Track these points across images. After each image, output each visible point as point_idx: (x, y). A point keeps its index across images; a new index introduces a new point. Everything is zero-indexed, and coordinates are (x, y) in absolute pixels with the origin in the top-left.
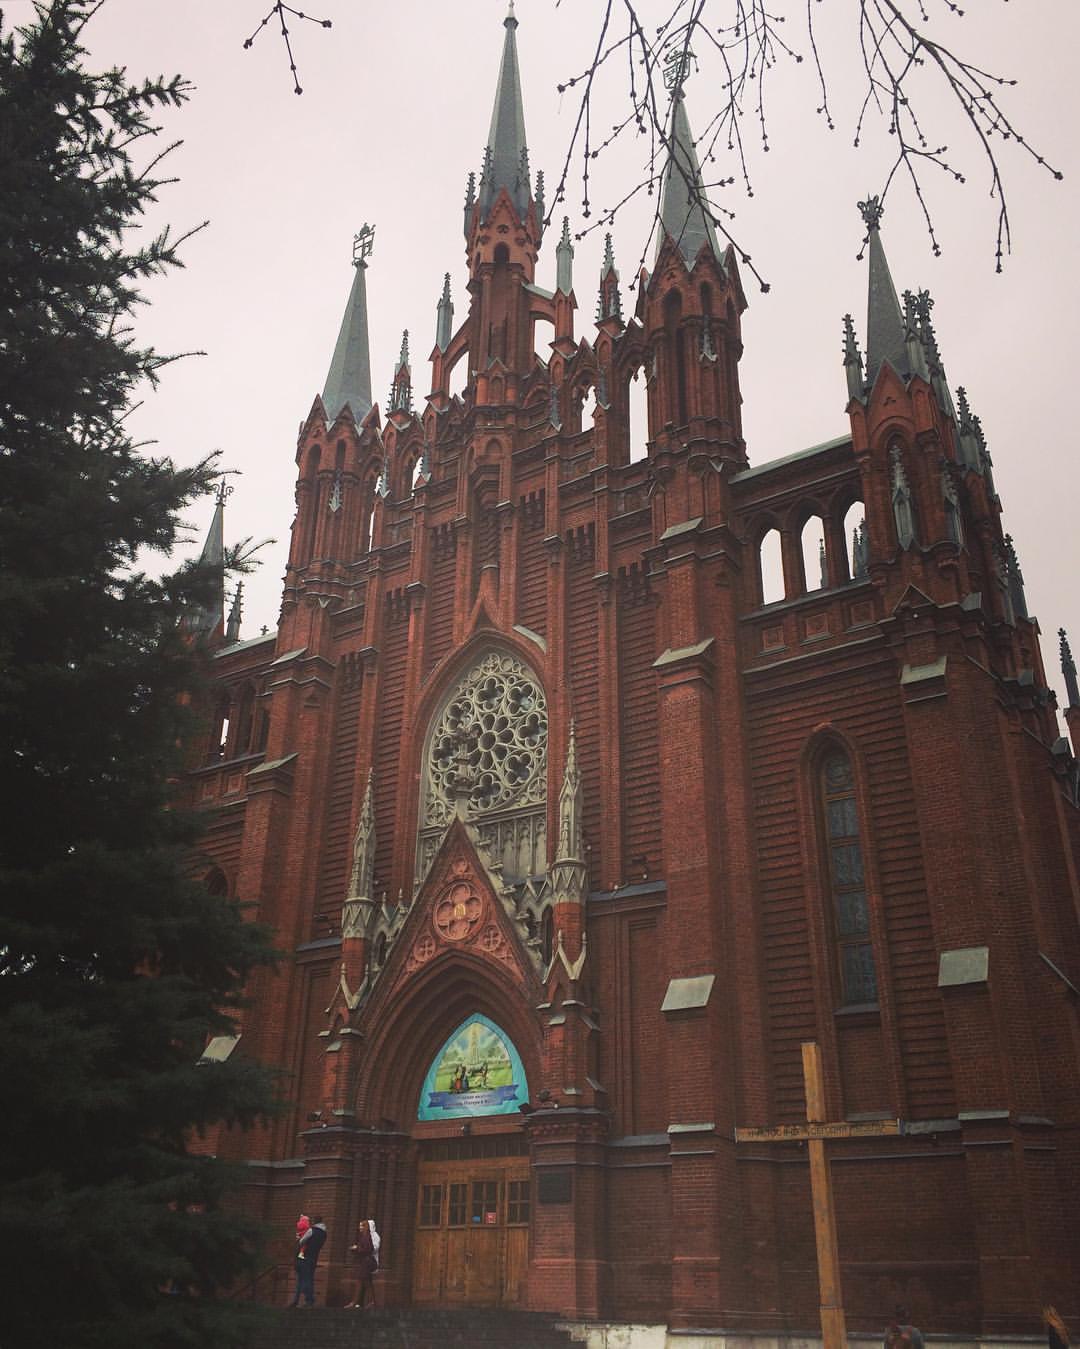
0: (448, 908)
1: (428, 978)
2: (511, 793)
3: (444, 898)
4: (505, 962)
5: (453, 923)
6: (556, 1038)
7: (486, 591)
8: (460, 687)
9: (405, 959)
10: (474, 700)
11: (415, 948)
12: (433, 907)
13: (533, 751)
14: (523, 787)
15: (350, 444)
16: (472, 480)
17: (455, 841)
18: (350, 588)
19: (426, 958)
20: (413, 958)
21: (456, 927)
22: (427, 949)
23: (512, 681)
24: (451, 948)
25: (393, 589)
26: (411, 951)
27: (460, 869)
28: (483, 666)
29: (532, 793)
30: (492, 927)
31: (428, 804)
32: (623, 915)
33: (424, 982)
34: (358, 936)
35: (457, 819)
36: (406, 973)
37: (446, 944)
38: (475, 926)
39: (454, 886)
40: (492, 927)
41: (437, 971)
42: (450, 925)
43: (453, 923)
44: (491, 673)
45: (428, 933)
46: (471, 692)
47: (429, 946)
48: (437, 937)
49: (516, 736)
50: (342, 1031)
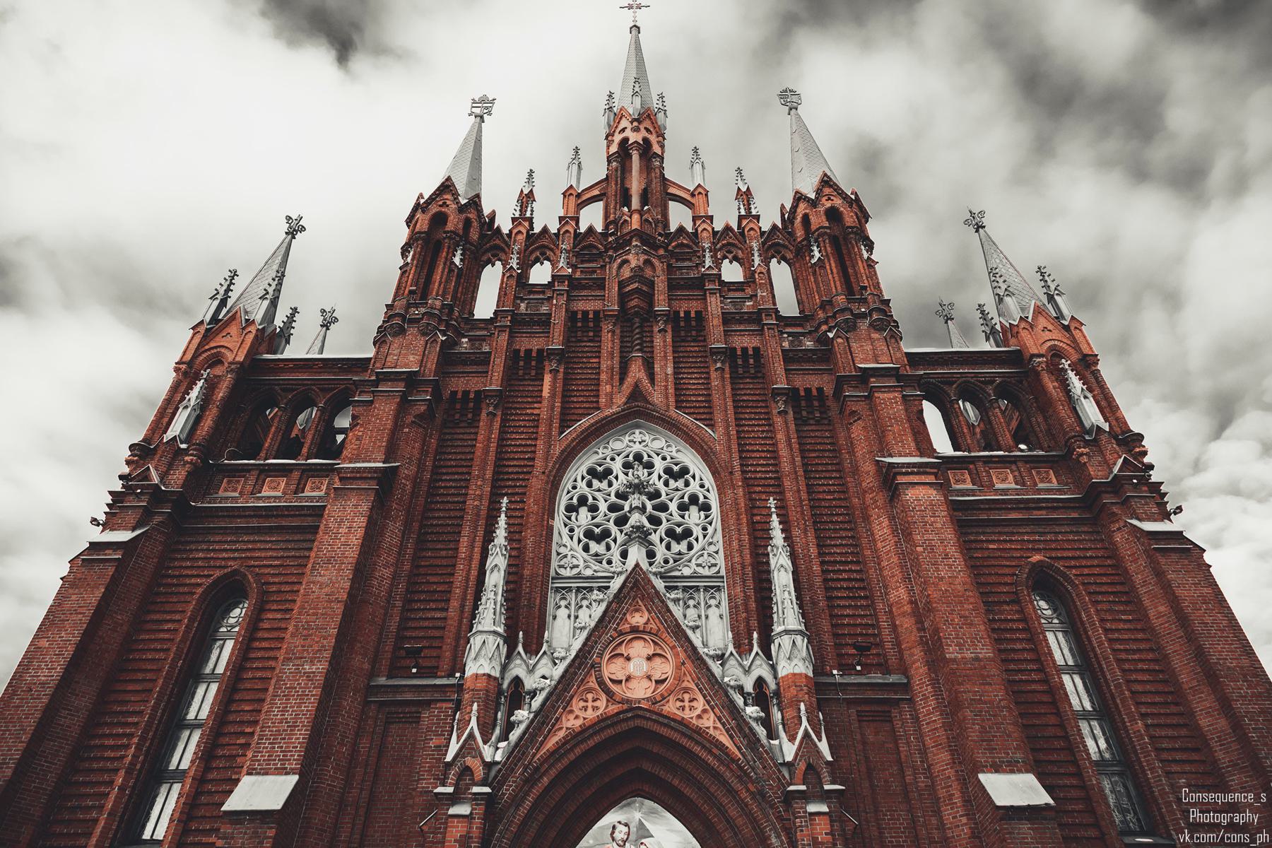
1: (597, 739)
4: (711, 732)
5: (628, 679)
6: (822, 830)
7: (637, 372)
8: (600, 451)
10: (617, 467)
11: (574, 701)
12: (601, 655)
13: (698, 525)
14: (687, 557)
15: (475, 224)
16: (621, 285)
17: (632, 588)
18: (465, 337)
19: (590, 714)
20: (571, 712)
21: (632, 684)
22: (590, 704)
23: (664, 459)
24: (632, 710)
25: (523, 349)
26: (569, 703)
27: (638, 619)
28: (627, 438)
29: (698, 565)
30: (686, 690)
31: (558, 554)
32: (850, 702)
33: (591, 743)
34: (493, 674)
35: (637, 565)
36: (561, 728)
37: (622, 701)
38: (662, 687)
39: (630, 637)
40: (686, 690)
41: (611, 732)
42: (627, 680)
43: (628, 679)
44: (637, 448)
45: (592, 683)
46: (613, 459)
47: (594, 700)
48: (610, 694)
49: (673, 507)
50: (476, 789)
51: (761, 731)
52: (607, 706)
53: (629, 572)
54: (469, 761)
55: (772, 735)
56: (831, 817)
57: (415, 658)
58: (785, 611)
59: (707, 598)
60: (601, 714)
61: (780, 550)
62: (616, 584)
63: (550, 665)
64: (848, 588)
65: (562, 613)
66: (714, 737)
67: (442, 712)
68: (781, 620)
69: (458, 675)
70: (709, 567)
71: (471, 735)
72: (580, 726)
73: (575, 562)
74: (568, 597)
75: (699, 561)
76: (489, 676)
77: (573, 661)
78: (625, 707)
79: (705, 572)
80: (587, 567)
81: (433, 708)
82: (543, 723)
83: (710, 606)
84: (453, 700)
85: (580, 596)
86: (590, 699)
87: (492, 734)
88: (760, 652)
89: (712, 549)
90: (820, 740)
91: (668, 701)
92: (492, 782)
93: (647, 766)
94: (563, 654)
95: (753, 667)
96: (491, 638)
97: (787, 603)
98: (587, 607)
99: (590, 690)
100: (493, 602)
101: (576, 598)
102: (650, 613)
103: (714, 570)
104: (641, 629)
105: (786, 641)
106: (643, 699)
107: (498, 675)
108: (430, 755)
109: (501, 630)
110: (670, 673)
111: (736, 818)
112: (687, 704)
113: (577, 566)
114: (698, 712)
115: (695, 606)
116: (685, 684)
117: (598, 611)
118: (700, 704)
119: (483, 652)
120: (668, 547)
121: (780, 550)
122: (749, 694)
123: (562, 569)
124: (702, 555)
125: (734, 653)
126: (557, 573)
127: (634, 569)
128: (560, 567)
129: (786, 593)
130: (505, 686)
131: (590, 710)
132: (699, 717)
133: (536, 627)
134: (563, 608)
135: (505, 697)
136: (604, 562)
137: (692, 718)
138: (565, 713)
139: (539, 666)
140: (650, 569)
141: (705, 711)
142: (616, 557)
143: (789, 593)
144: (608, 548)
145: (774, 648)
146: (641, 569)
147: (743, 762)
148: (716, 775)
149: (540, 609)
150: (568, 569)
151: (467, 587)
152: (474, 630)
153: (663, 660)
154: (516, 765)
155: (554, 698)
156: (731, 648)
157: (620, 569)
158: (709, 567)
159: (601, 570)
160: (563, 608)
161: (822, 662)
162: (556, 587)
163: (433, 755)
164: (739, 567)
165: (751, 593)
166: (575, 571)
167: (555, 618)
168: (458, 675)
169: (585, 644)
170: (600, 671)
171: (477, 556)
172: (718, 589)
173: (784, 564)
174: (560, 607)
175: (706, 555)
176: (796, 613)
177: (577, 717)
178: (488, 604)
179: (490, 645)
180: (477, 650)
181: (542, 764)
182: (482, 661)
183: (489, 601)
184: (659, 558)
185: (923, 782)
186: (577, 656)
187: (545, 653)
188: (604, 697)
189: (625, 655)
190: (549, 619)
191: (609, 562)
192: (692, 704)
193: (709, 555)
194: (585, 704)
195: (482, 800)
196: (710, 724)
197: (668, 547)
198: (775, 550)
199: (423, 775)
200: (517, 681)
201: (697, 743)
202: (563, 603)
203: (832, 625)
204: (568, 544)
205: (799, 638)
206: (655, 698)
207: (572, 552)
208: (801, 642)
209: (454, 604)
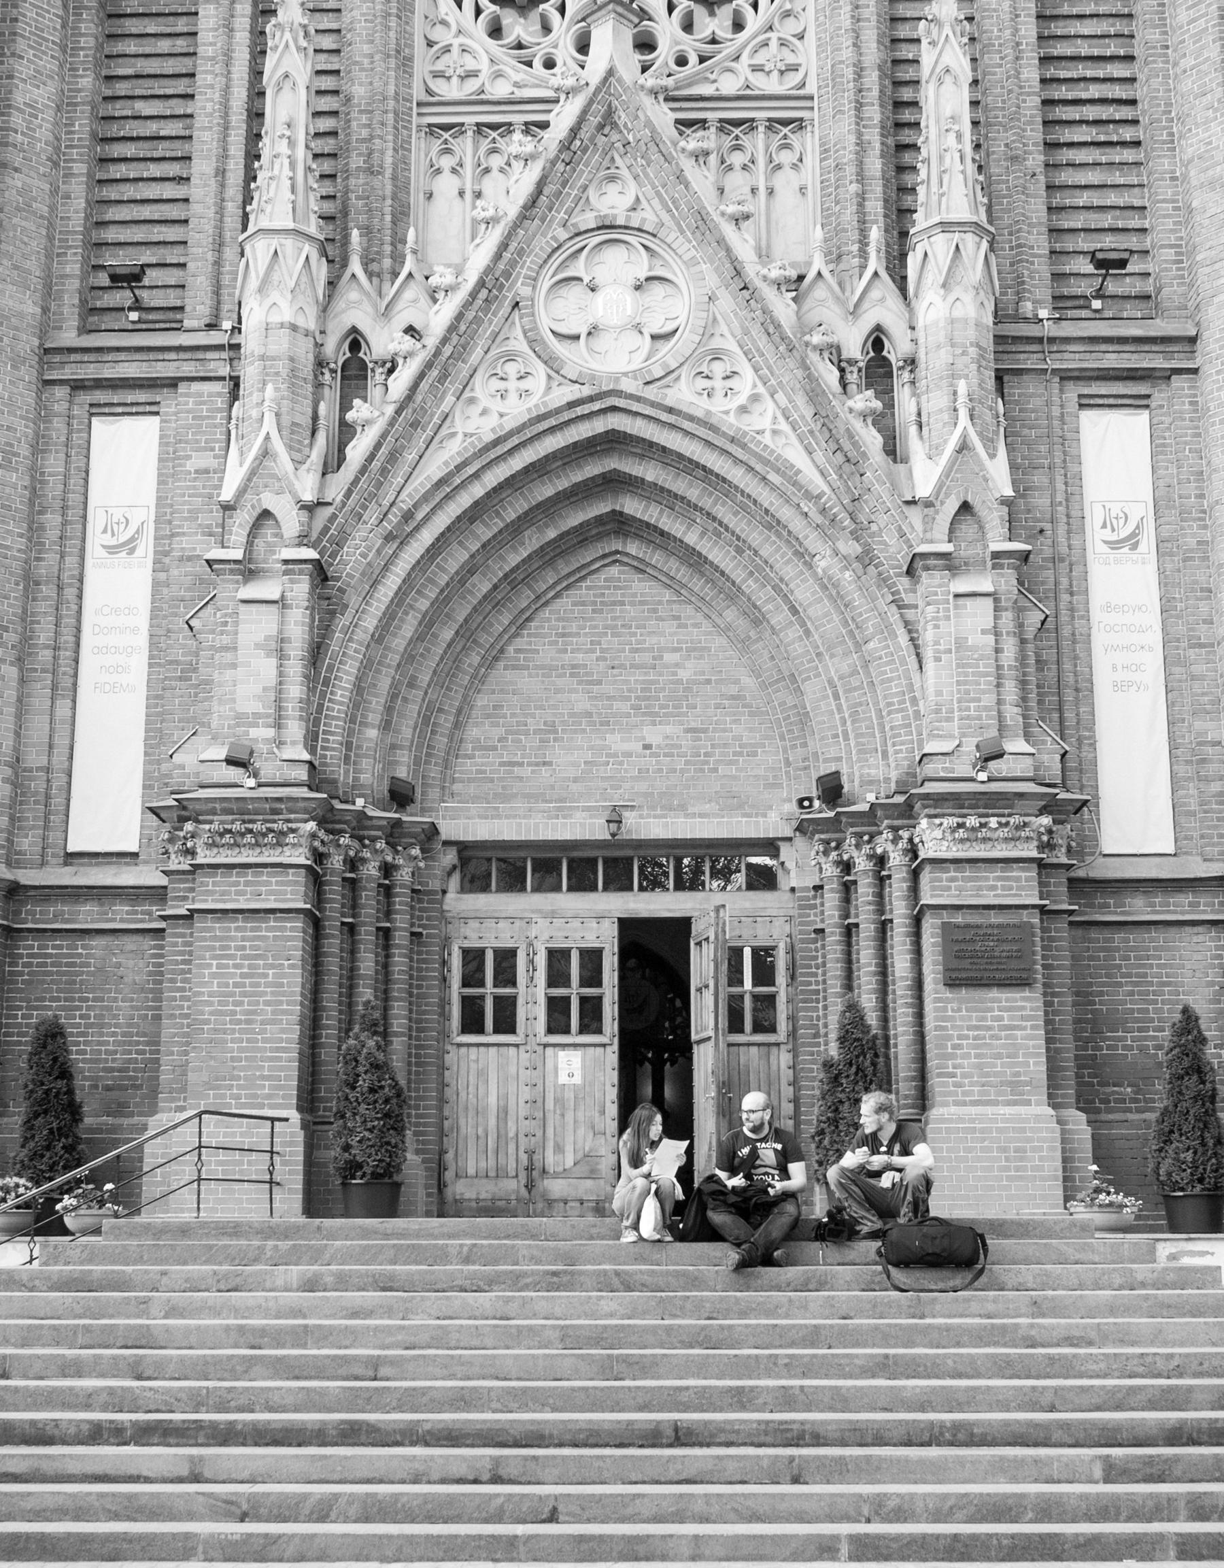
0: (575, 291)
2: (693, 59)
3: (563, 265)
4: (767, 439)
9: (450, 399)
14: (728, 50)
17: (601, 127)
21: (602, 342)
22: (512, 385)
29: (756, 69)
31: (430, 44)
34: (301, 322)
35: (610, 72)
36: (453, 435)
38: (665, 347)
42: (589, 334)
45: (519, 344)
48: (551, 362)
51: (872, 440)
52: (549, 388)
53: (592, 88)
54: (269, 501)
55: (892, 450)
56: (996, 600)
57: (132, 288)
58: (946, 178)
59: (773, 148)
60: (536, 406)
61: (947, 30)
62: (563, 118)
63: (424, 300)
64: (1097, 122)
65: (446, 185)
66: (773, 451)
67: (204, 403)
68: (935, 198)
69: (227, 325)
70: (782, 73)
71: (265, 453)
72: (493, 430)
73: (470, 64)
74: (456, 148)
75: (759, 59)
76: (294, 328)
77: (473, 295)
78: (586, 391)
79: (771, 85)
80: (498, 75)
81: (182, 395)
82: (415, 425)
83: (779, 167)
84: (223, 379)
85: (485, 145)
86: (513, 375)
87: (311, 445)
88: (883, 274)
89: (789, 28)
90: (992, 456)
91: (678, 378)
92: (319, 540)
93: (632, 506)
94: (449, 279)
95: (866, 305)
96: (289, 243)
97: (951, 159)
98: (502, 170)
99: (510, 358)
100: (286, 162)
101: (476, 149)
102: (640, 185)
103: (794, 79)
104: (620, 221)
105: (941, 247)
106: (625, 374)
107: (312, 325)
108: (188, 488)
109: (313, 227)
110: (682, 320)
111: (810, 605)
112: (718, 384)
113: (473, 74)
114: (742, 399)
115: (745, 167)
116: (716, 343)
117: (525, 180)
118: (747, 383)
119: (276, 277)
120: (688, 27)
121: (947, 30)
122: (852, 362)
123: (440, 81)
124: (765, 44)
125: (826, 273)
126: (429, 92)
127: (605, 79)
128: (437, 75)
129: (952, 137)
130: (329, 349)
131: (513, 397)
132: (743, 410)
133: (388, 218)
134: (447, 173)
135: (333, 371)
136: (538, 63)
137: (727, 412)
138: (460, 403)
139: (400, 305)
140: (641, 81)
141: (755, 398)
142: (565, 52)
143: (959, 136)
144: (546, 29)
145: (913, 261)
146: (620, 81)
147: (829, 499)
148: (773, 524)
149: (394, 178)
150: (455, 80)
151: (226, 127)
152: (251, 228)
153: (668, 288)
154: (365, 508)
155: (435, 373)
156: (818, 264)
157: (570, 82)
158: (782, 73)
159: (537, 83)
160: (447, 173)
161: (1018, 293)
162: (430, 125)
163: (194, 487)
164: (849, 73)
165: (874, 137)
166: (472, 85)
167: (430, 196)
168: (227, 325)
169: (498, 256)
170: (533, 315)
171: (242, 56)
172: (799, 124)
173: (954, 65)
174: (439, 171)
175: (774, 44)
176: (970, 184)
177: (484, 412)
178: (277, 167)
179: (290, 262)
180: (261, 273)
181: (416, 506)
182: (275, 296)
183: (277, 162)
184: (664, 53)
185: (1194, 535)
186: (481, 284)
187: (410, 275)
188: (540, 370)
189: (586, 280)
190: (416, 198)
191: (549, 64)
192: (729, 383)
193: (783, 43)
194: (501, 385)
195: (301, 572)
196: (765, 423)
197: (688, 27)
198: (935, 31)
199: (179, 527)
200: (355, 341)
201: (737, 461)
202: (446, 162)
203: (1049, 209)
204: (450, 19)
205: (970, 239)
206: (649, 372)
207: (462, 39)
208: (975, 249)
209: (202, 167)
